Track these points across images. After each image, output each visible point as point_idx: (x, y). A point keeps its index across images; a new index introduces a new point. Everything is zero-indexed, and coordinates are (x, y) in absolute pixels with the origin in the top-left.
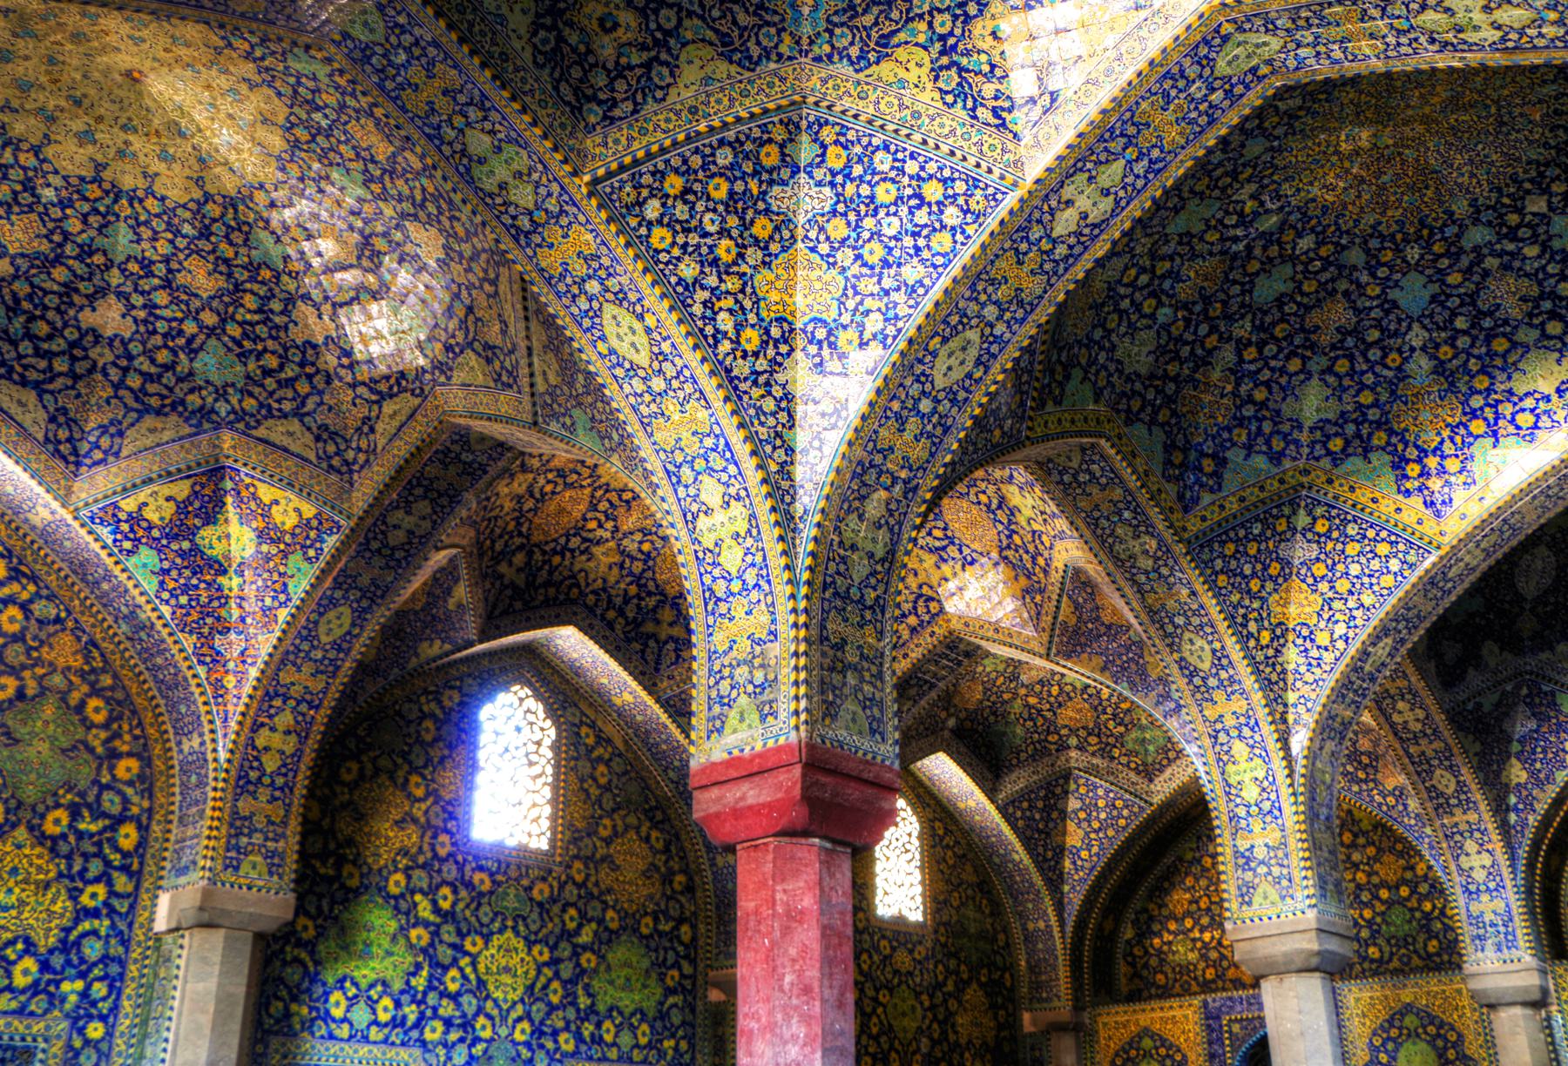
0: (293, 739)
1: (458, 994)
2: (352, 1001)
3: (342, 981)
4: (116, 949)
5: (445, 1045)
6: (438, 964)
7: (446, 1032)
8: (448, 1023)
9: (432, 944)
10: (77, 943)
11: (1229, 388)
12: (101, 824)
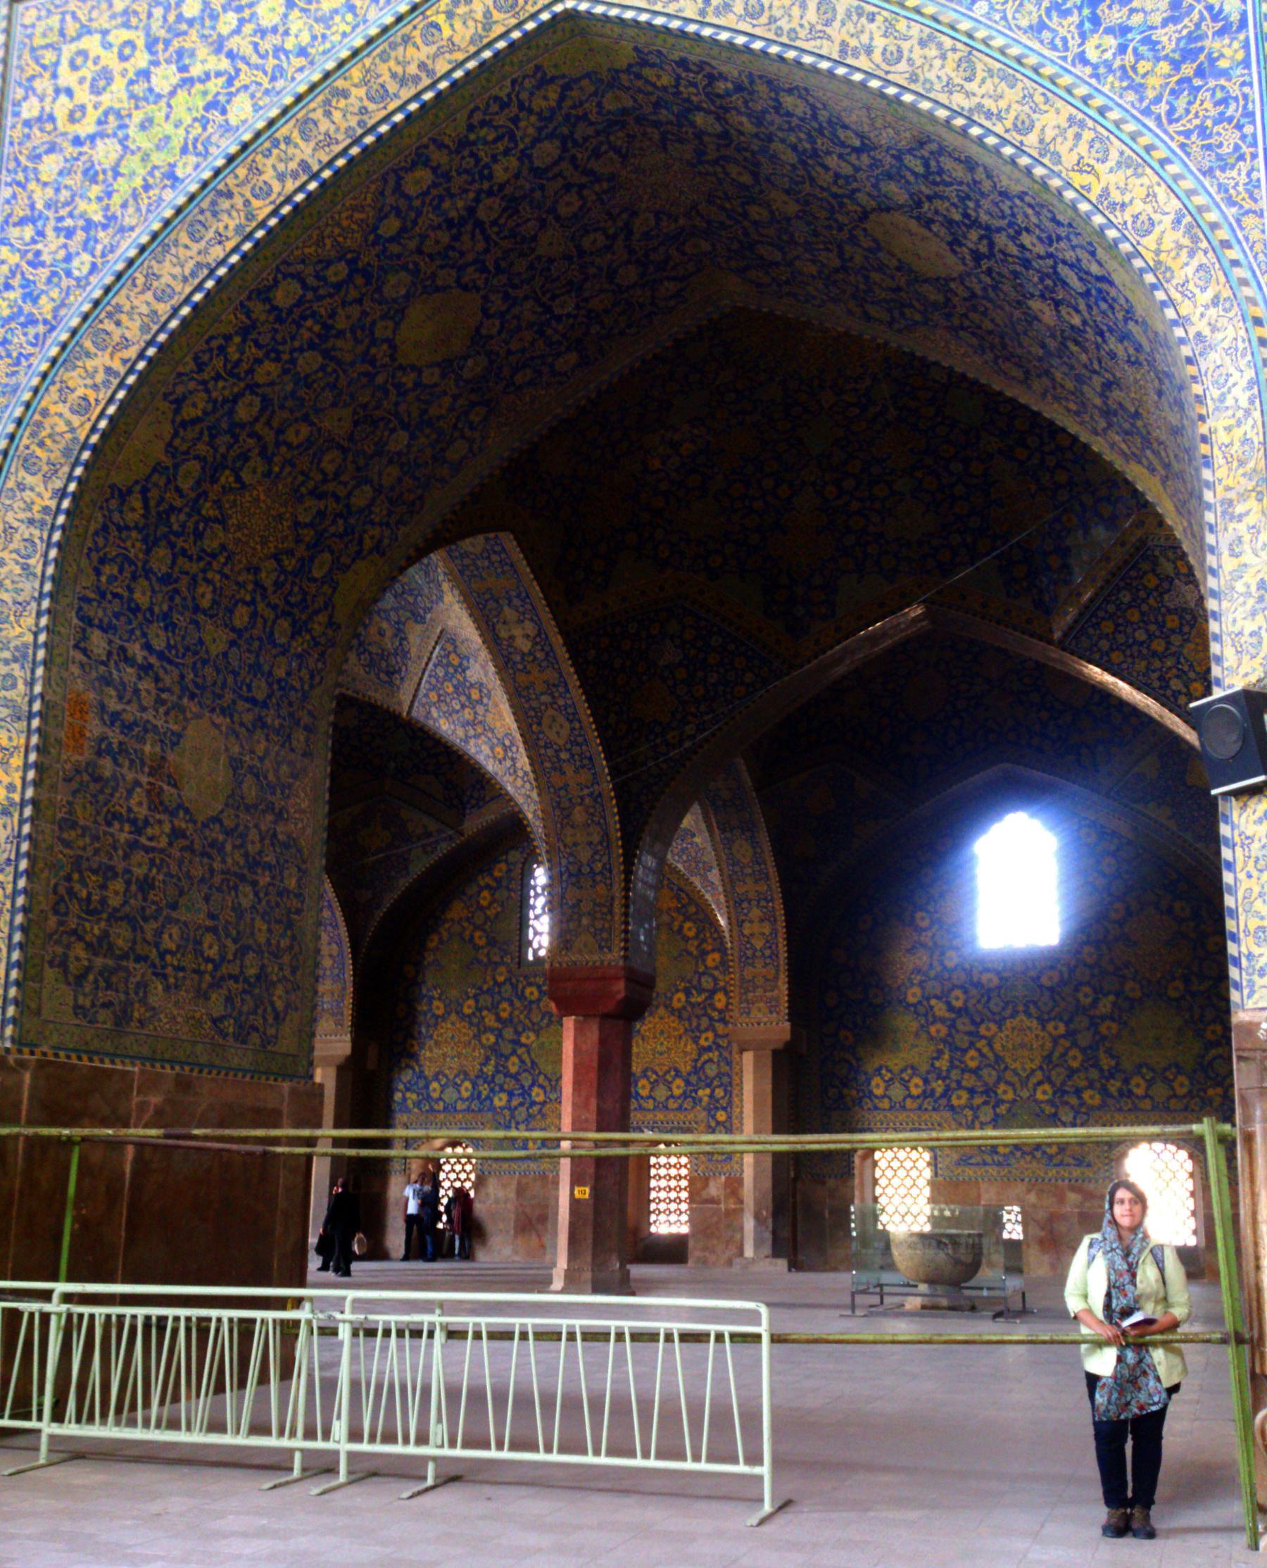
0: (766, 924)
1: (979, 1068)
2: (889, 1083)
3: (880, 1068)
4: (726, 1069)
5: (971, 1108)
6: (957, 1049)
7: (971, 1098)
8: (972, 1091)
9: (950, 1035)
10: (702, 1067)
11: (1033, 488)
12: (703, 996)
